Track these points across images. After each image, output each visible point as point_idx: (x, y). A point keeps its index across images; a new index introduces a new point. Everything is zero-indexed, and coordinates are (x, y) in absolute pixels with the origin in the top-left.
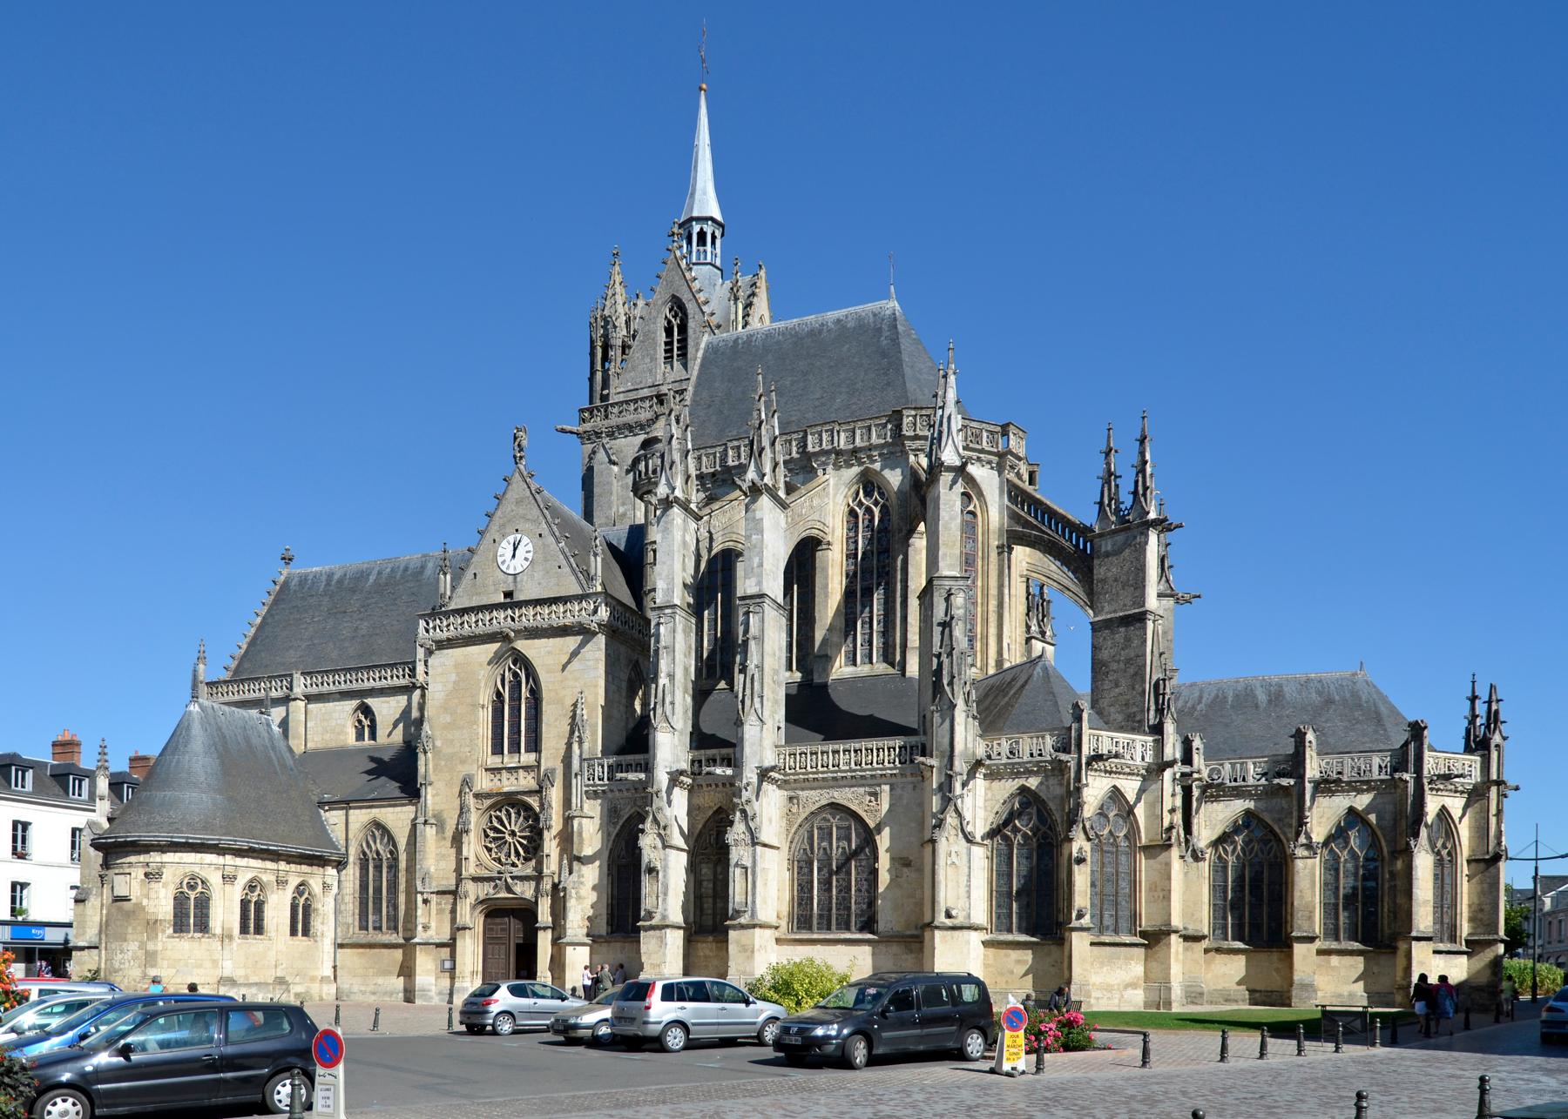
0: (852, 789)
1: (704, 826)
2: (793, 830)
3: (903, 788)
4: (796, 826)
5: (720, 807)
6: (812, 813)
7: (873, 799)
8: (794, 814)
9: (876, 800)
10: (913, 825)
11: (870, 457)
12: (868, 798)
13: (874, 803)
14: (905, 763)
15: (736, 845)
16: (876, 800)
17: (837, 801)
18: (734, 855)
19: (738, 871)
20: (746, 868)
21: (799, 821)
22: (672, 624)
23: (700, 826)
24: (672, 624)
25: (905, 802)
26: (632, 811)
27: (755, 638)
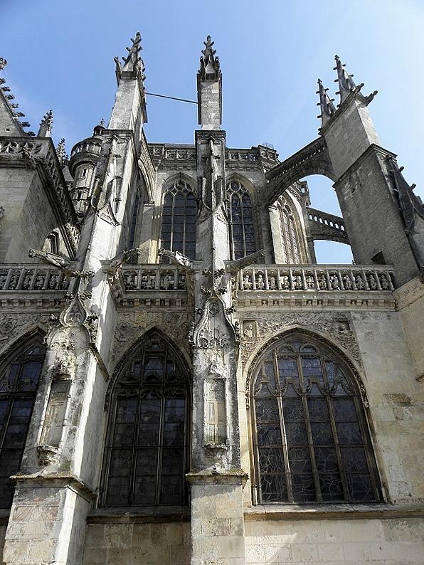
0: (318, 316)
1: (130, 350)
2: (251, 358)
3: (376, 317)
4: (255, 353)
5: (154, 329)
6: (273, 340)
7: (343, 326)
8: (250, 339)
9: (348, 329)
10: (399, 356)
11: (237, 167)
12: (337, 325)
13: (347, 332)
14: (377, 289)
15: (205, 347)
16: (348, 329)
17: (304, 328)
18: (202, 360)
19: (208, 387)
20: (223, 381)
21: (258, 347)
22: (125, 144)
23: (126, 349)
24: (125, 144)
25: (382, 331)
26: (34, 326)
27: (216, 157)
